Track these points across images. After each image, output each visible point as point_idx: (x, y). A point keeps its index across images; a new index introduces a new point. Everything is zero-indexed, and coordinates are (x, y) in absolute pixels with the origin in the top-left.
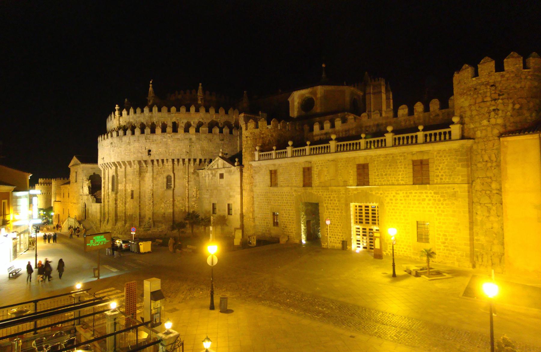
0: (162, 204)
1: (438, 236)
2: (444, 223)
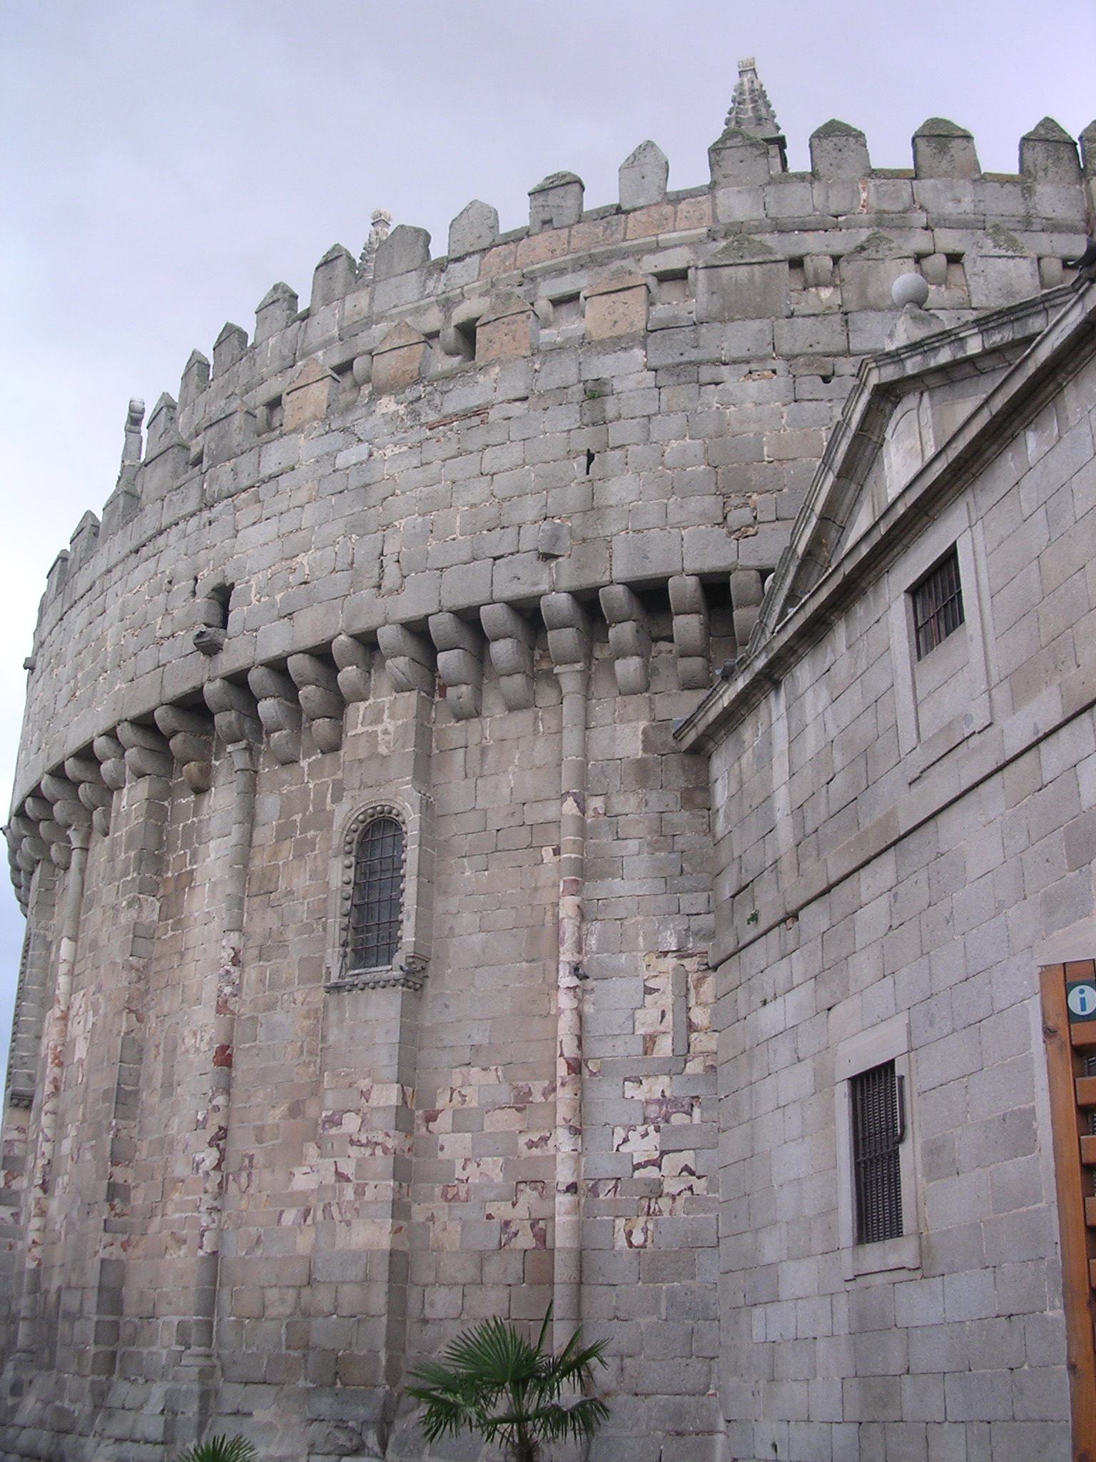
0: (300, 1158)
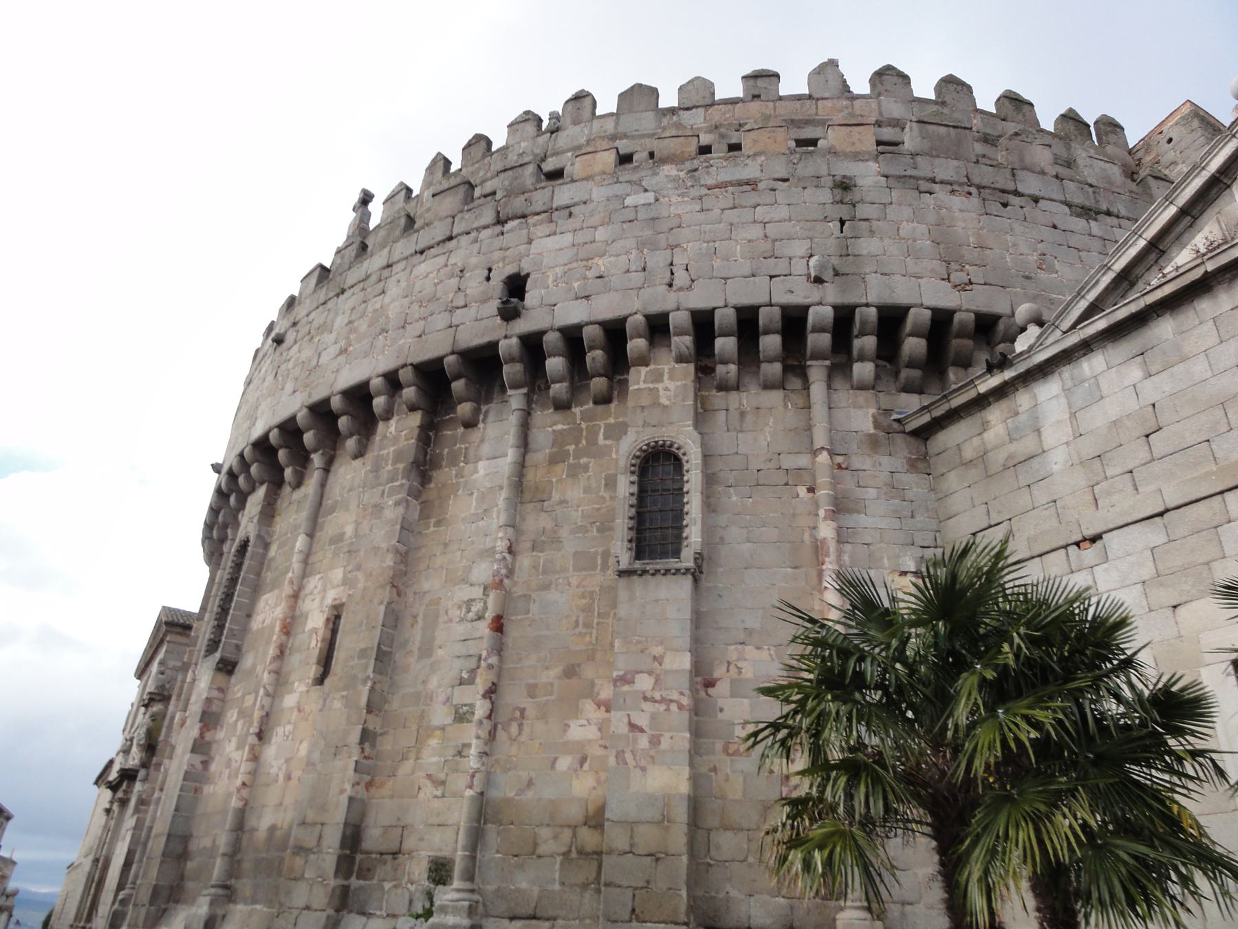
0: (576, 712)
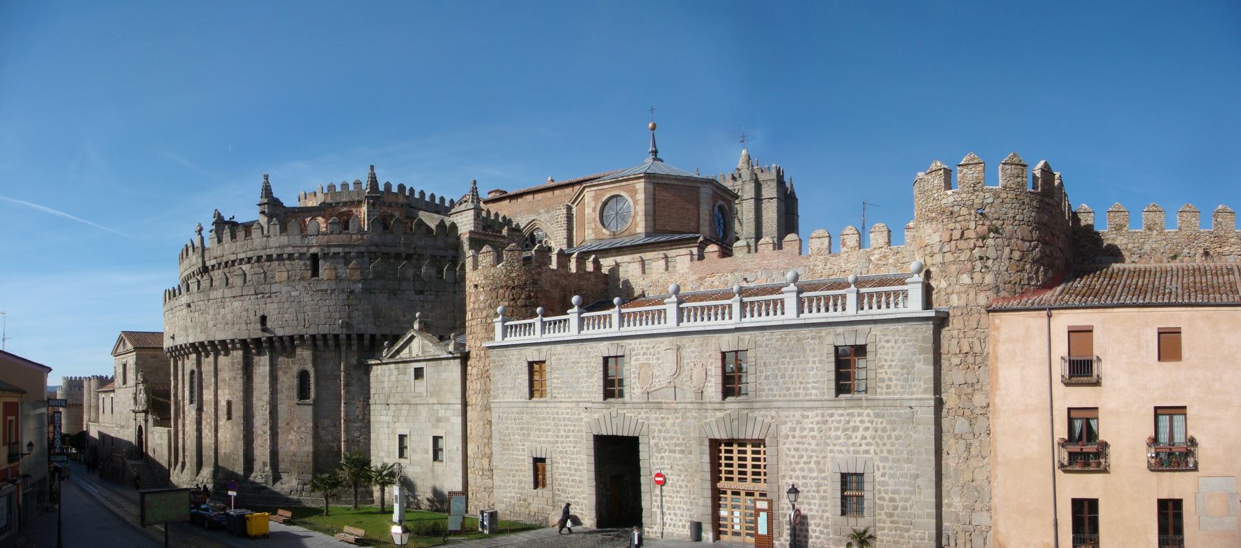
0: (290, 433)
1: (881, 502)
2: (891, 476)
